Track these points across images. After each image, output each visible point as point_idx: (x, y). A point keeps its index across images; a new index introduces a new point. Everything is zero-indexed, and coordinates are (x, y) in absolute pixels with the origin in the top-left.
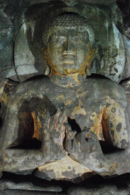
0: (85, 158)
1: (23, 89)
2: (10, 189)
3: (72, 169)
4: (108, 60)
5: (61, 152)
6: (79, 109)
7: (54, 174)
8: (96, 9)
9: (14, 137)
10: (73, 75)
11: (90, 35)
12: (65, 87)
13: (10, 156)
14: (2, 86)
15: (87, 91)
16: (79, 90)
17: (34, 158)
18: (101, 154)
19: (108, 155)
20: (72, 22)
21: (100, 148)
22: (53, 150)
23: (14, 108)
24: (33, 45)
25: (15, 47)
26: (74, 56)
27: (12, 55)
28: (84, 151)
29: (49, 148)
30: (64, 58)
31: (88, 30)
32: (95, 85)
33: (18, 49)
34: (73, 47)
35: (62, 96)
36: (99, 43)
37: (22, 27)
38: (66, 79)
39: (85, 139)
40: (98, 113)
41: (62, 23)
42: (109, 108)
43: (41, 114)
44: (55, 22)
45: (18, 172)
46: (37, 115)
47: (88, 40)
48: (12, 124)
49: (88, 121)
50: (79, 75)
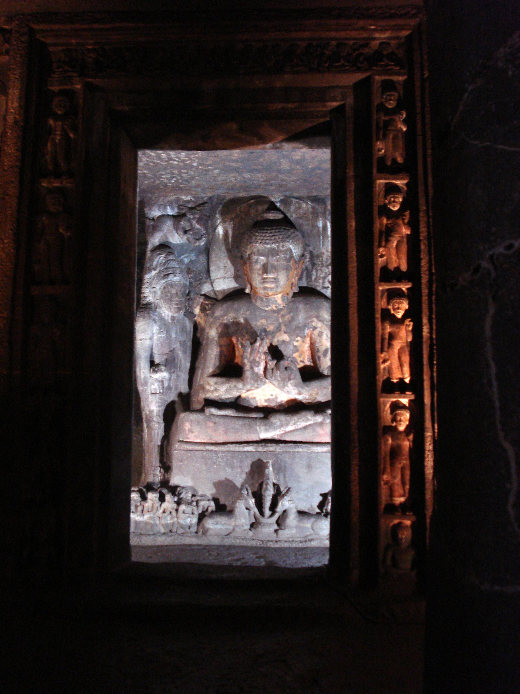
0: (284, 386)
1: (222, 312)
2: (215, 415)
3: (274, 397)
4: (321, 270)
5: (261, 380)
6: (281, 335)
7: (256, 401)
8: (307, 204)
9: (214, 365)
10: (275, 296)
11: (293, 251)
12: (267, 309)
13: (212, 384)
14: (198, 305)
15: (292, 314)
16: (282, 313)
17: (235, 386)
18: (299, 382)
19: (308, 383)
20: (273, 238)
21: (299, 376)
22: (253, 379)
23: (213, 333)
24: (231, 253)
25: (210, 256)
26: (275, 279)
27: (206, 266)
28: (283, 380)
29: (250, 377)
30: (264, 282)
31: (291, 246)
32: (301, 306)
33: (214, 259)
34: (274, 267)
35: (264, 321)
36: (311, 248)
37: (217, 231)
38: (268, 300)
39: (284, 368)
40: (304, 337)
41: (263, 240)
42: (316, 332)
43: (242, 340)
44: (254, 238)
45: (221, 399)
46: (238, 340)
47: (292, 257)
48: (212, 351)
49: (291, 347)
50: (283, 296)
